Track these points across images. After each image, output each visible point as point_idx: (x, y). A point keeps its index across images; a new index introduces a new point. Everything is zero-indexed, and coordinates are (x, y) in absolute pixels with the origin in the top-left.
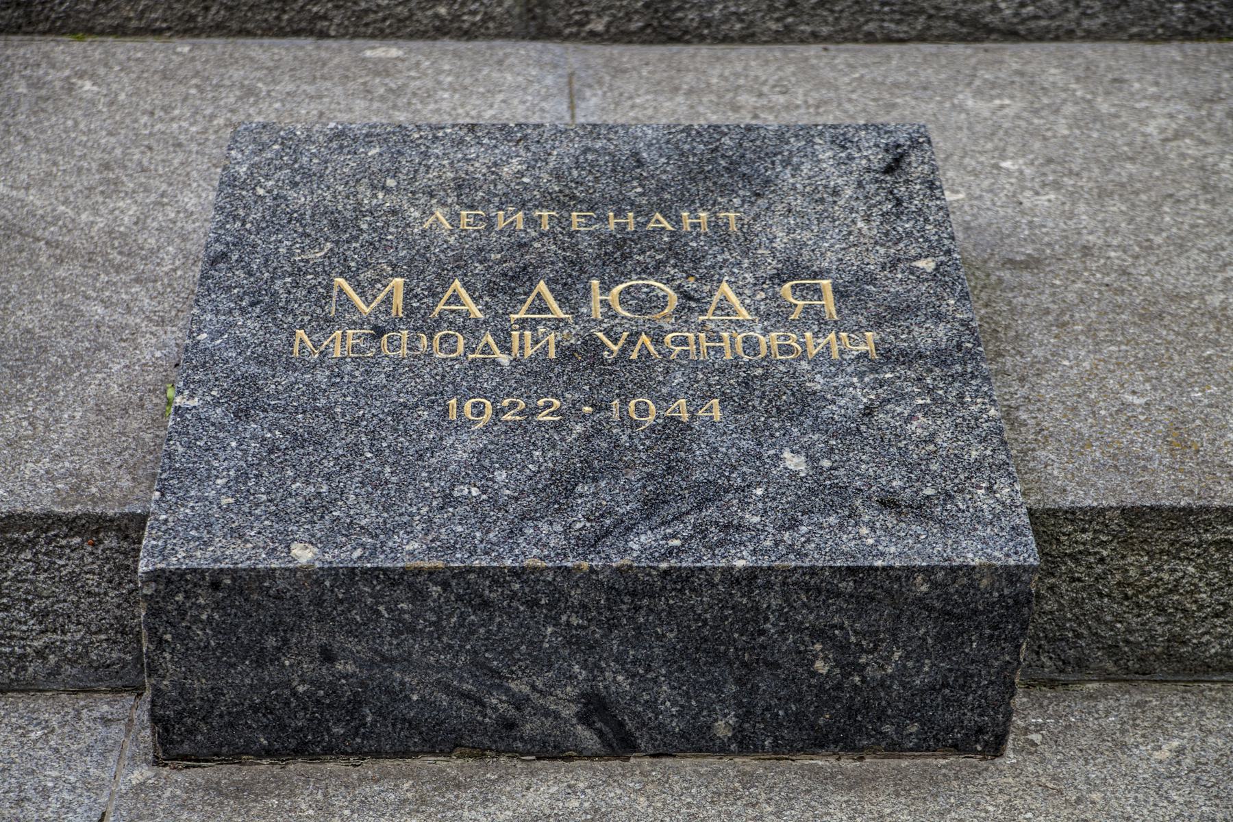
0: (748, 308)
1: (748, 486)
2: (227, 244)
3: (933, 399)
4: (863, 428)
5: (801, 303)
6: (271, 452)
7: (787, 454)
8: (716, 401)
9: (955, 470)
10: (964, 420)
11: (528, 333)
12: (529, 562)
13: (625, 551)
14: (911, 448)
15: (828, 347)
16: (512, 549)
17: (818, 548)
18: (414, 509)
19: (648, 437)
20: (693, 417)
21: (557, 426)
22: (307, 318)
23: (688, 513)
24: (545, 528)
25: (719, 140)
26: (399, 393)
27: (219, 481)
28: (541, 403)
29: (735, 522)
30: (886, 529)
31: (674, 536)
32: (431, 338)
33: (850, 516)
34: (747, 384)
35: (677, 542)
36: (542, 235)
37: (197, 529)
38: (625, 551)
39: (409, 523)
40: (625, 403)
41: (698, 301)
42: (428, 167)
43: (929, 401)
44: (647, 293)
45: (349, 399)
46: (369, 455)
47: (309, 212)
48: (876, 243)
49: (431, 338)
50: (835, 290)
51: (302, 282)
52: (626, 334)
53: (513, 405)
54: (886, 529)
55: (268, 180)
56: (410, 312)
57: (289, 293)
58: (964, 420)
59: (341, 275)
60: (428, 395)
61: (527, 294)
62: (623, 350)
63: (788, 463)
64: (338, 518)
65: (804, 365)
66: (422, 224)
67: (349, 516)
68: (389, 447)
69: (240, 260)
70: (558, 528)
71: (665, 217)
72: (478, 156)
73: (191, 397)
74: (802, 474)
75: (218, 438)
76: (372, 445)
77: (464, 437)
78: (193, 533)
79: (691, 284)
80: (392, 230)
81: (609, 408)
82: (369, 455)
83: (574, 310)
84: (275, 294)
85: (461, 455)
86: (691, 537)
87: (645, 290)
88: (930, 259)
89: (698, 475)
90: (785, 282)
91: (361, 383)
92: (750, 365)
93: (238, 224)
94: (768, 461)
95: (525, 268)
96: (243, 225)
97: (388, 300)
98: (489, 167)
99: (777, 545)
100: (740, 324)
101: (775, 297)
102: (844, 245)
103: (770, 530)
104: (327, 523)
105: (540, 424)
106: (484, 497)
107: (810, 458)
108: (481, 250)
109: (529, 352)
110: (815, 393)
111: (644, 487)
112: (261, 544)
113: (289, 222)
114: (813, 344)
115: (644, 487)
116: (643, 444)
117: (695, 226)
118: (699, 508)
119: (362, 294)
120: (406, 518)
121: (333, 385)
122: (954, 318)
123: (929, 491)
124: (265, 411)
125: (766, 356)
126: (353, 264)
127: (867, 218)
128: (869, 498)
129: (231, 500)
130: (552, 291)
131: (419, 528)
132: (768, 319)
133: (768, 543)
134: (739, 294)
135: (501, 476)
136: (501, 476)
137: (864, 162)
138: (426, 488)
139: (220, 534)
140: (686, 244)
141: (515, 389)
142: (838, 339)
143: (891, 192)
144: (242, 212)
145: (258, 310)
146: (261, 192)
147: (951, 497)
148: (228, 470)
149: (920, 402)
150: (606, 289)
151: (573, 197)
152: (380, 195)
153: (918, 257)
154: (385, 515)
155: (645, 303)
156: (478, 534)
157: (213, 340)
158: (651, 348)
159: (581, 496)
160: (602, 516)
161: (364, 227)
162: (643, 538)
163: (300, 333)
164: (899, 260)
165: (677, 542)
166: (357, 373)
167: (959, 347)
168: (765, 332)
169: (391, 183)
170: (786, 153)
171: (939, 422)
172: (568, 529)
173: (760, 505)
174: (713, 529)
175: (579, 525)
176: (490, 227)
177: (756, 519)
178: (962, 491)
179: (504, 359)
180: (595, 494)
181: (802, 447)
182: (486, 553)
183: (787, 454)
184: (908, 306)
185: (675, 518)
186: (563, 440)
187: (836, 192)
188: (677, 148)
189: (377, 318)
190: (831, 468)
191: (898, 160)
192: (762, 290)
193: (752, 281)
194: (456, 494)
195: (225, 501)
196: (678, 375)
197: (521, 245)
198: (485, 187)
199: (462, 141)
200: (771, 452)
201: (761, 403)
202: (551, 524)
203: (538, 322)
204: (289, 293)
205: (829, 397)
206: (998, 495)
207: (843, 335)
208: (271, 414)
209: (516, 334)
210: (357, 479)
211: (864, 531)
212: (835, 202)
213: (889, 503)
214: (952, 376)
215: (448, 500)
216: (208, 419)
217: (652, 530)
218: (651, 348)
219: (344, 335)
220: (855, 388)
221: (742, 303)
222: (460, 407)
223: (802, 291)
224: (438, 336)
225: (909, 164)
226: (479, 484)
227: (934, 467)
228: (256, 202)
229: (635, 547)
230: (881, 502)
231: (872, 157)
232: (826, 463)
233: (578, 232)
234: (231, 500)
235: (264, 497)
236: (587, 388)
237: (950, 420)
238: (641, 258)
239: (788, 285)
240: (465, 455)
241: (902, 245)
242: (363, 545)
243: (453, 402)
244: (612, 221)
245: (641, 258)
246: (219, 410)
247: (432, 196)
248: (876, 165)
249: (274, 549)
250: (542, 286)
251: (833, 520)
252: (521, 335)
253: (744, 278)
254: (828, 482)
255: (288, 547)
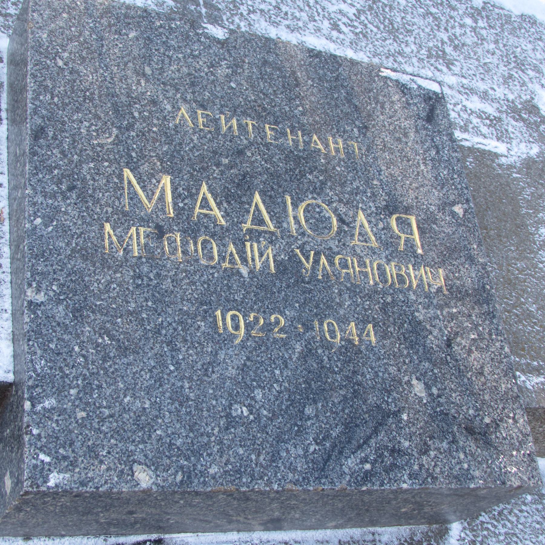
0: (375, 235)
1: (399, 411)
2: (43, 118)
3: (478, 335)
4: (448, 357)
5: (403, 236)
6: (104, 360)
7: (414, 382)
8: (370, 326)
9: (496, 400)
10: (495, 355)
11: (255, 245)
12: (289, 486)
13: (342, 475)
14: (474, 378)
15: (421, 280)
16: (276, 475)
17: (442, 472)
18: (209, 429)
19: (339, 360)
20: (360, 340)
21: (285, 343)
22: (110, 210)
23: (370, 437)
24: (293, 451)
25: (338, 70)
26: (182, 299)
27: (72, 392)
28: (273, 318)
29: (397, 447)
30: (472, 455)
31: (364, 460)
32: (195, 244)
33: (453, 442)
34: (385, 310)
35: (368, 466)
36: (251, 144)
37: (64, 447)
38: (342, 475)
39: (207, 445)
40: (321, 324)
41: (348, 225)
42: (170, 58)
43: (476, 337)
44: (319, 213)
45: (150, 304)
46: (172, 368)
47: (96, 92)
48: (432, 186)
49: (195, 244)
50: (419, 228)
51: (102, 170)
52: (312, 253)
53: (256, 319)
54: (472, 455)
55: (64, 51)
56: (179, 211)
57: (94, 179)
58: (495, 355)
59: (127, 165)
60: (202, 304)
61: (250, 204)
62: (313, 268)
63: (416, 389)
64: (160, 438)
65: (413, 297)
66: (174, 118)
67: (168, 436)
68: (184, 359)
69: (55, 138)
70: (301, 452)
71: (319, 139)
72: (200, 54)
73: (38, 291)
74: (425, 401)
75: (63, 340)
76: (173, 357)
77: (230, 352)
78: (61, 451)
79: (342, 209)
80: (155, 121)
81: (312, 329)
82: (172, 368)
83: (279, 224)
84: (84, 180)
85: (232, 372)
86: (375, 460)
87: (318, 210)
88: (460, 205)
89: (372, 399)
90: (392, 214)
91: (155, 287)
92: (385, 293)
93: (49, 96)
94: (405, 386)
95: (244, 176)
96: (52, 98)
97: (162, 198)
98: (209, 68)
99: (420, 468)
100: (373, 251)
101: (387, 228)
102: (416, 185)
103: (416, 455)
104: (154, 442)
105: (275, 341)
106: (252, 417)
107: (428, 387)
108: (215, 152)
109: (258, 265)
110: (420, 323)
111: (343, 410)
112: (112, 465)
113: (84, 101)
114: (414, 275)
115: (343, 410)
116: (337, 366)
117: (337, 150)
118: (376, 432)
119: (144, 188)
120: (205, 439)
121: (138, 286)
122: (478, 262)
123: (487, 420)
124: (93, 312)
125: (391, 285)
126: (134, 154)
127: (425, 164)
128: (460, 425)
129: (84, 414)
130: (264, 202)
131: (215, 449)
132: (387, 249)
133: (416, 467)
134: (370, 222)
135: (258, 394)
136: (258, 394)
137: (415, 109)
138: (214, 407)
139: (81, 453)
140: (334, 168)
141: (255, 303)
142: (426, 273)
143: (432, 140)
144: (49, 83)
145: (74, 196)
146: (60, 63)
147: (498, 425)
148: (76, 378)
149: (473, 337)
150: (295, 206)
151: (264, 109)
152: (143, 82)
153: (454, 203)
154: (191, 435)
155: (319, 223)
156: (253, 457)
157: (47, 226)
158: (328, 268)
159: (309, 418)
160: (324, 439)
161: (136, 114)
162: (349, 461)
163: (108, 227)
164: (445, 203)
165: (368, 466)
166: (152, 276)
167: (484, 287)
168: (388, 261)
169: (148, 70)
170: (375, 91)
171: (484, 356)
172: (306, 451)
173: (407, 429)
174: (386, 453)
175: (312, 449)
176: (218, 129)
177: (407, 444)
178: (501, 420)
179: (244, 271)
180: (317, 416)
181: (421, 374)
182: (261, 478)
183: (414, 382)
184: (456, 247)
185: (365, 442)
186: (291, 358)
187: (406, 135)
188: (316, 71)
189: (157, 216)
190: (439, 396)
191: (432, 110)
192: (381, 219)
193: (373, 209)
194: (234, 414)
195: (81, 414)
196: (347, 296)
197: (241, 153)
198: (209, 87)
199: (188, 37)
200: (406, 378)
201: (395, 329)
202: (295, 447)
203: (260, 233)
204: (94, 179)
205: (428, 327)
206: (518, 425)
207: (428, 269)
208: (99, 316)
209: (248, 244)
210: (168, 395)
211: (462, 456)
212: (407, 143)
213: (470, 431)
214: (484, 314)
215: (231, 422)
216: (53, 317)
217: (353, 453)
218: (328, 268)
219: (138, 234)
220: (440, 320)
221: (372, 231)
222: (224, 319)
223: (402, 223)
224: (200, 240)
225: (438, 116)
226: (247, 403)
227: (487, 397)
228: (58, 74)
229: (347, 470)
230: (466, 429)
231: (419, 105)
232: (435, 391)
233: (271, 144)
234: (84, 414)
235: (107, 412)
236: (297, 305)
237: (488, 355)
238: (310, 177)
239: (394, 217)
240: (234, 372)
241: (445, 190)
242: (182, 467)
243: (218, 313)
244: (290, 137)
245: (310, 177)
246: (61, 308)
247: (177, 90)
248: (423, 114)
249: (122, 471)
250: (257, 198)
251: (445, 445)
252: (251, 246)
253: (370, 207)
254: (438, 409)
255: (131, 469)
